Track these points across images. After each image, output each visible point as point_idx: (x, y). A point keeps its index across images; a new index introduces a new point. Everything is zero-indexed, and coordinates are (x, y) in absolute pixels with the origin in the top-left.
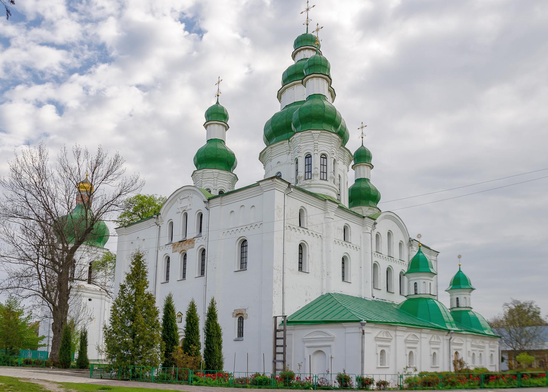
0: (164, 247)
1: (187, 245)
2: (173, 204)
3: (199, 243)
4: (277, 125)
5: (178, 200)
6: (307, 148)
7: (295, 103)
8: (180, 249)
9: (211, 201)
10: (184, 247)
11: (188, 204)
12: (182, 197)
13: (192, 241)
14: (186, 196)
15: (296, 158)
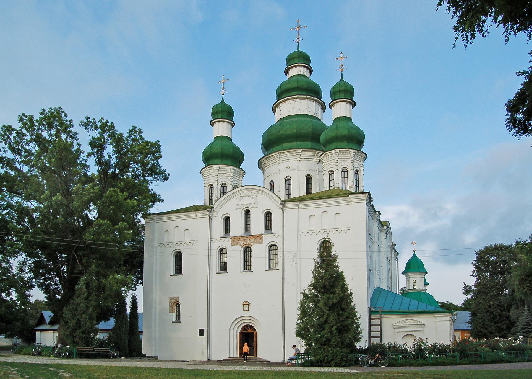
0: (218, 240)
1: (253, 239)
2: (230, 200)
3: (268, 240)
4: (286, 133)
5: (237, 197)
6: (344, 163)
7: (298, 115)
8: (242, 242)
9: (287, 204)
10: (248, 242)
11: (252, 202)
12: (242, 195)
13: (259, 237)
14: (250, 194)
15: (332, 171)
